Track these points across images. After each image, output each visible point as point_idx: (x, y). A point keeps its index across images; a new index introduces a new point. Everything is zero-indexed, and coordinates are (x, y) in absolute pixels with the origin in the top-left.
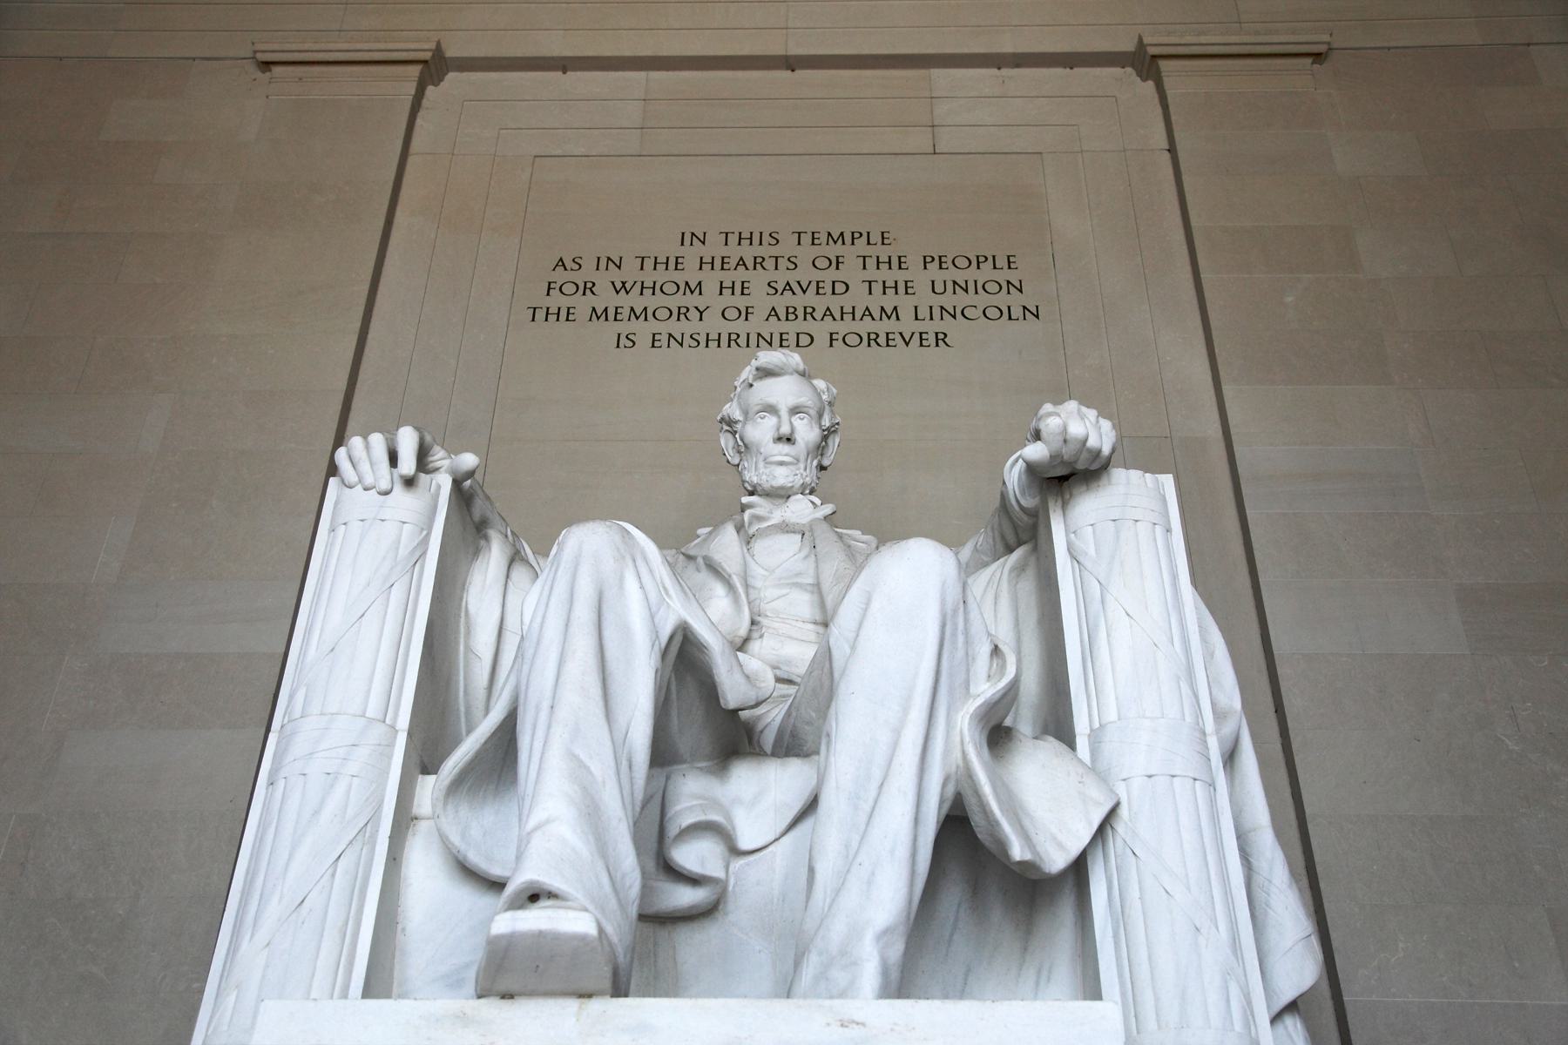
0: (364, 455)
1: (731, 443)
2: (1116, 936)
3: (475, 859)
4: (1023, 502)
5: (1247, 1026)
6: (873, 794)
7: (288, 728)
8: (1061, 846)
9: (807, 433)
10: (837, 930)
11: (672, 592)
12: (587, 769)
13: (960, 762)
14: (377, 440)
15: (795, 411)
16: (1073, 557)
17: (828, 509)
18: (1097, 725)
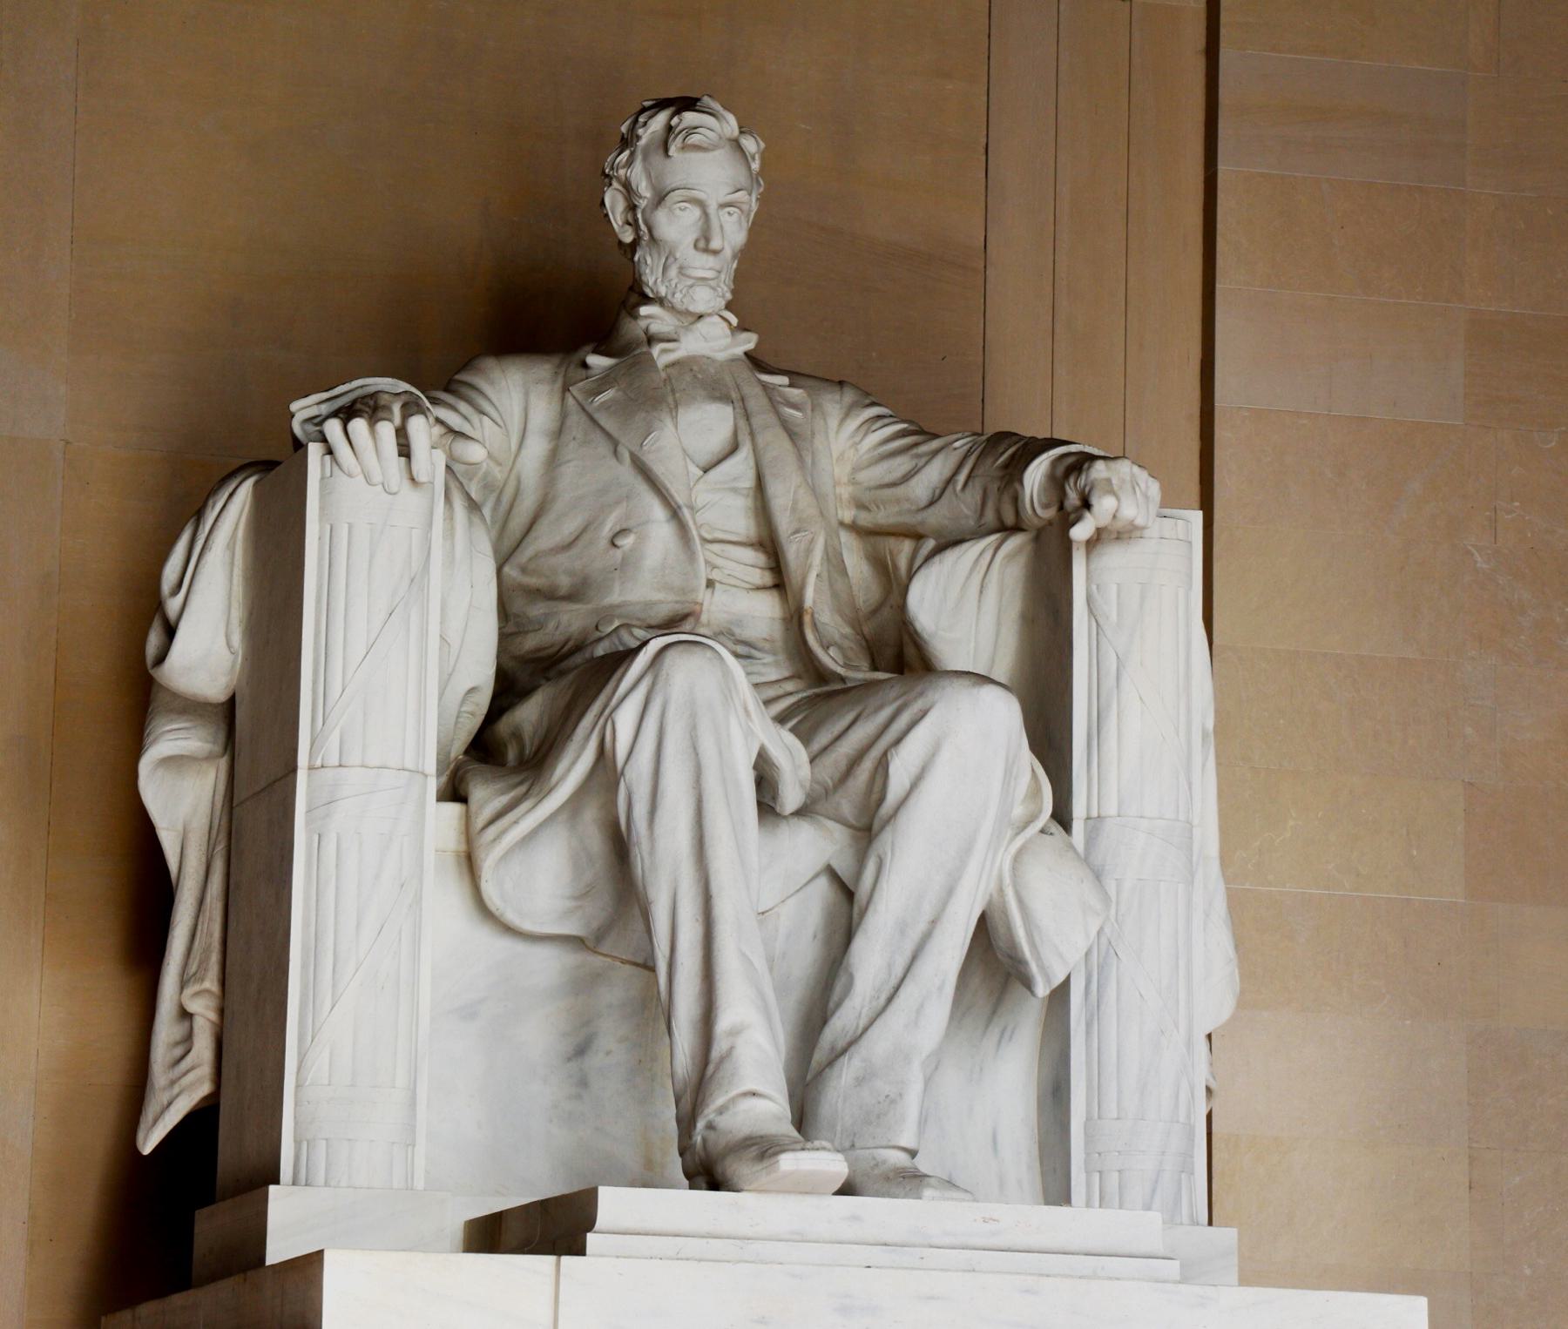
0: (370, 443)
1: (621, 205)
2: (1089, 1025)
3: (511, 917)
4: (1039, 511)
5: (1188, 1117)
6: (922, 926)
7: (328, 774)
8: (1061, 956)
9: (732, 233)
10: (879, 1043)
11: (754, 716)
12: (751, 963)
13: (995, 895)
14: (386, 430)
15: (723, 206)
16: (1091, 611)
17: (749, 341)
18: (1094, 814)
